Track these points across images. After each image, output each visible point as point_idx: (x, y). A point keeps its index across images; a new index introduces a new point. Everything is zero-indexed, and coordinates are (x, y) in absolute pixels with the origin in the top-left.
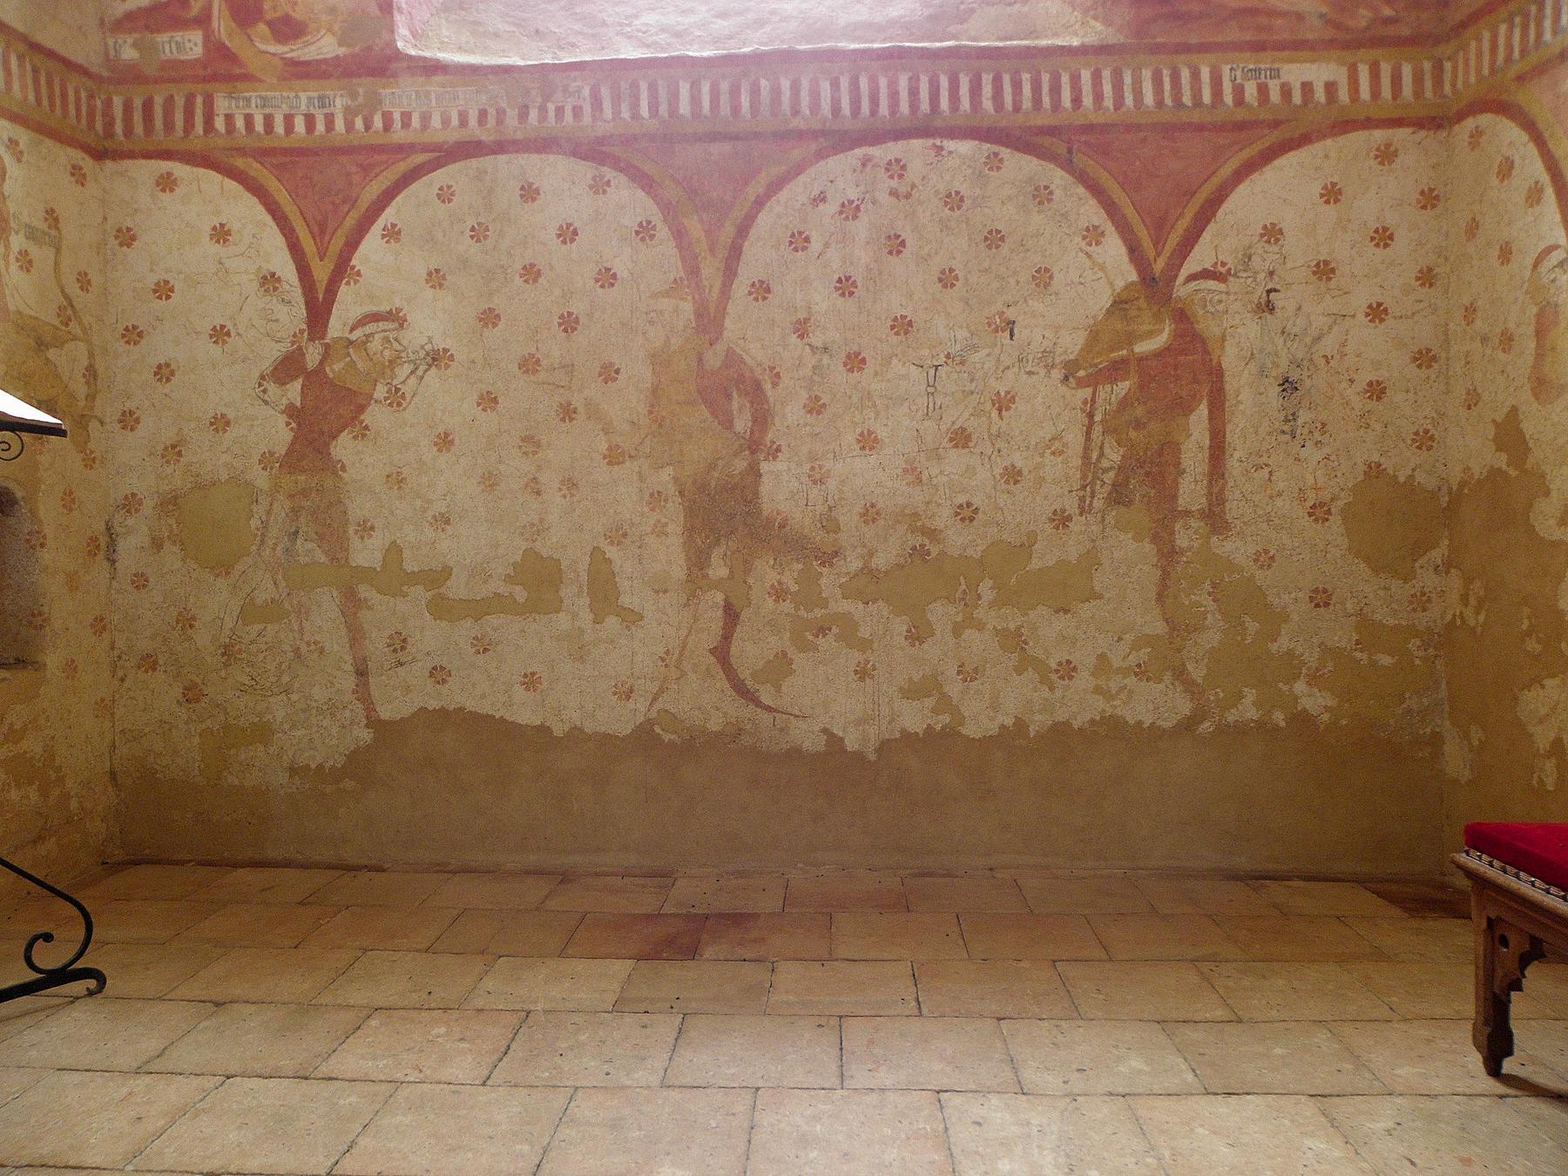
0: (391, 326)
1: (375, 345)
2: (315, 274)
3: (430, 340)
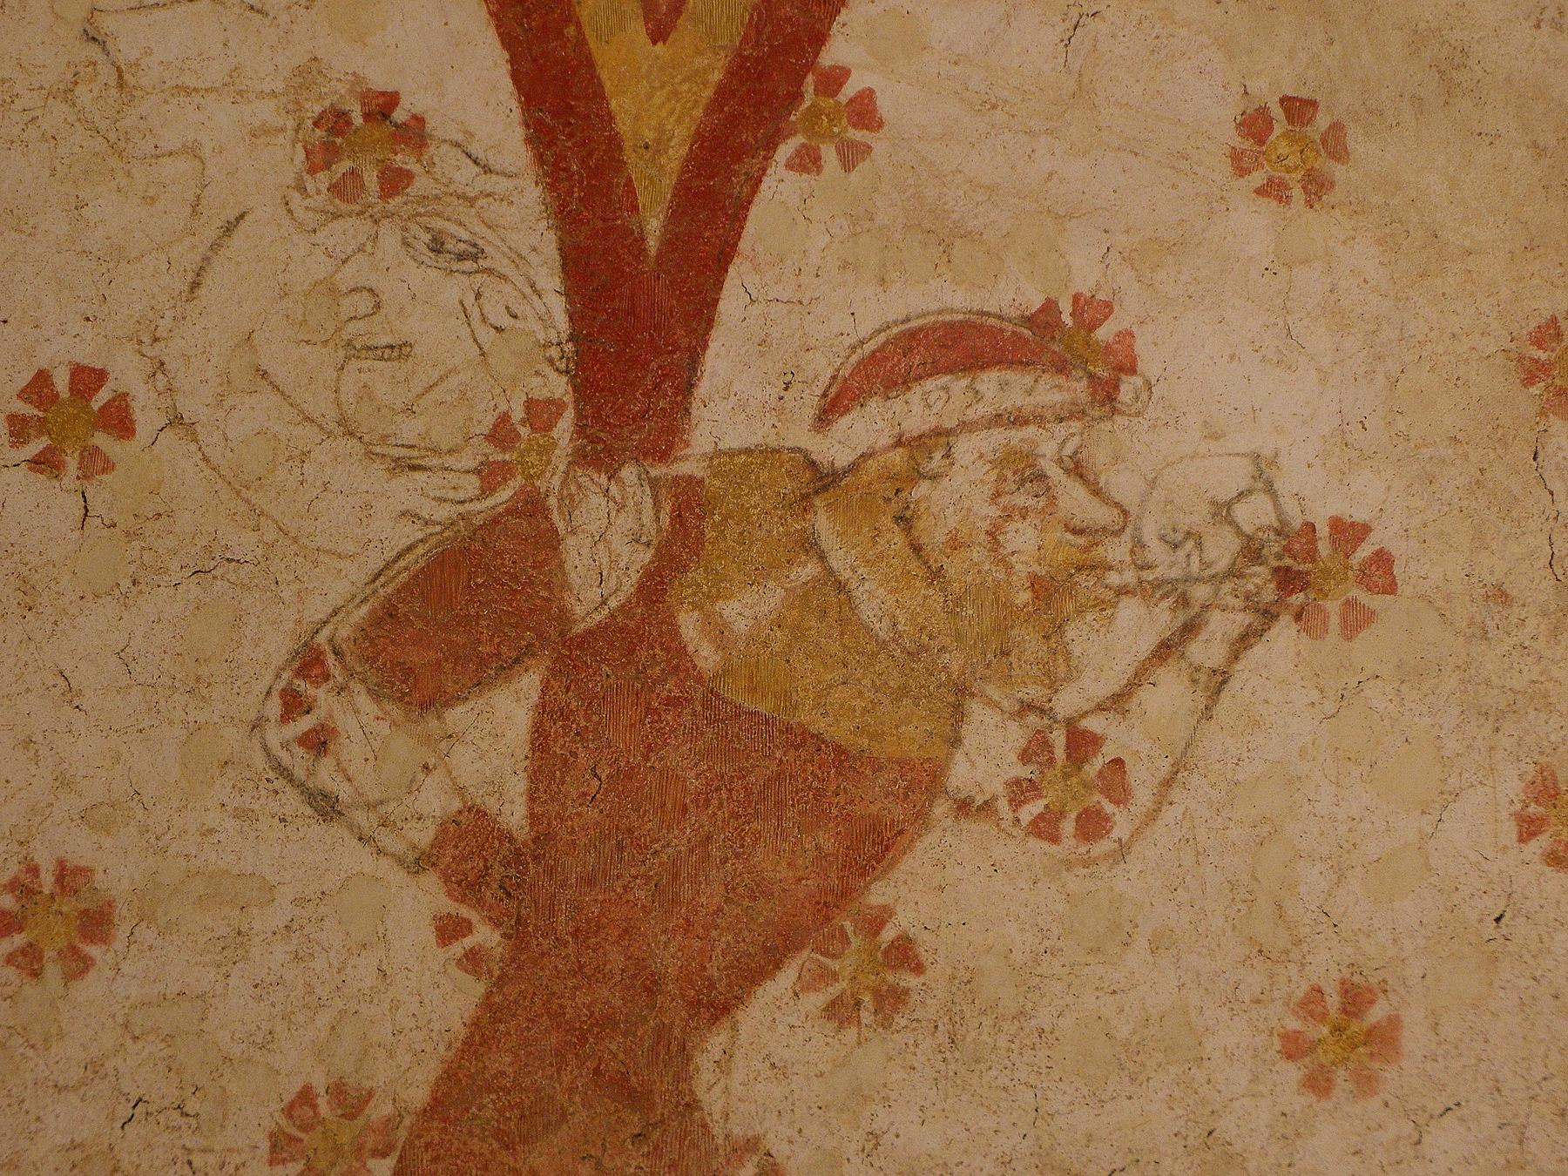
0: (1050, 392)
1: (959, 494)
2: (622, 106)
3: (1263, 476)
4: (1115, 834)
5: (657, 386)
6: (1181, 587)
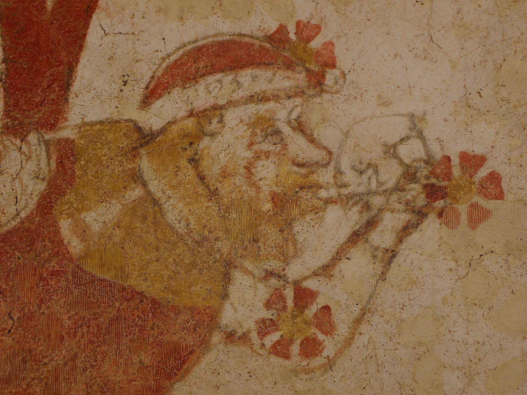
0: (282, 80)
1: (228, 144)
3: (416, 127)
4: (325, 353)
5: (49, 86)
6: (365, 198)
